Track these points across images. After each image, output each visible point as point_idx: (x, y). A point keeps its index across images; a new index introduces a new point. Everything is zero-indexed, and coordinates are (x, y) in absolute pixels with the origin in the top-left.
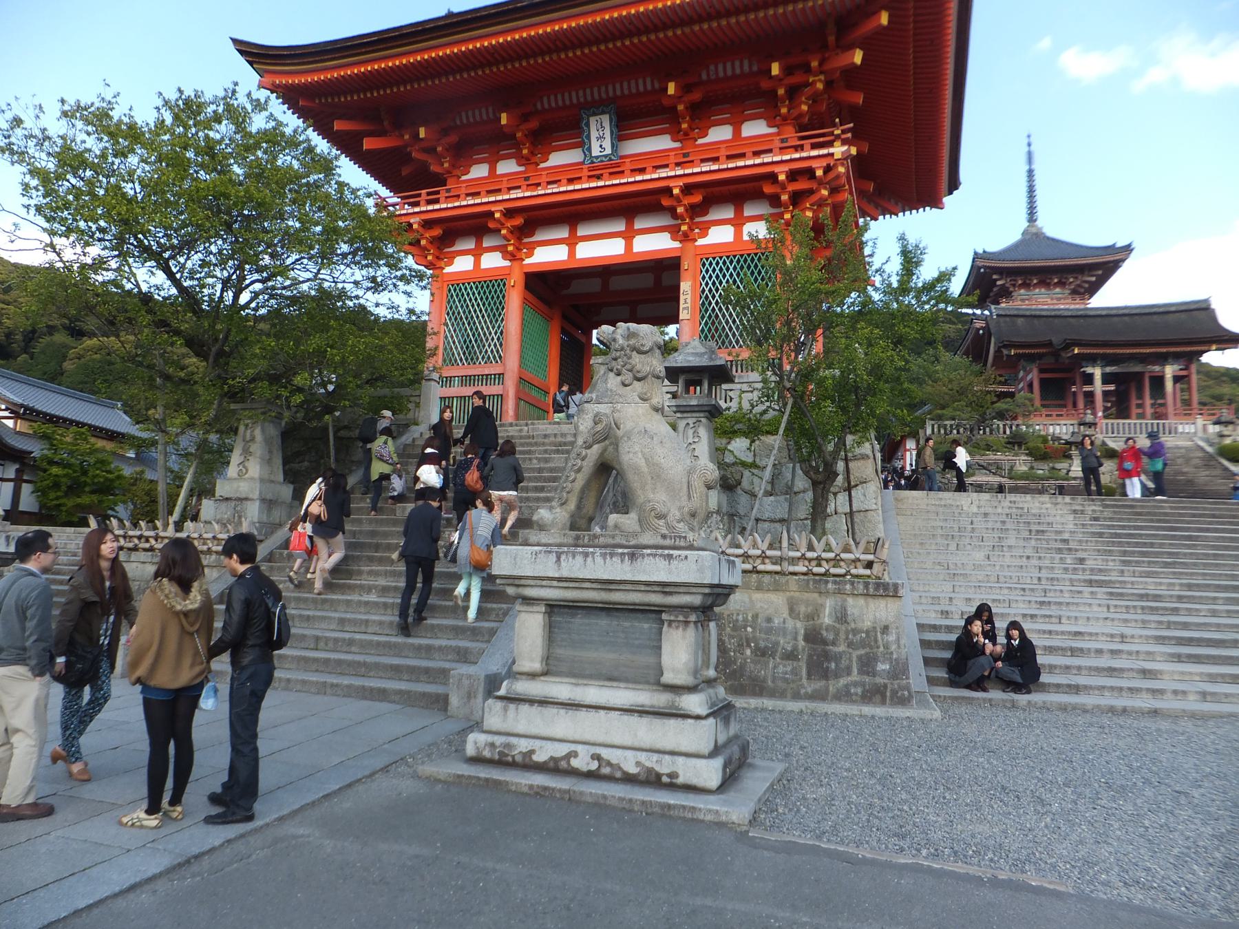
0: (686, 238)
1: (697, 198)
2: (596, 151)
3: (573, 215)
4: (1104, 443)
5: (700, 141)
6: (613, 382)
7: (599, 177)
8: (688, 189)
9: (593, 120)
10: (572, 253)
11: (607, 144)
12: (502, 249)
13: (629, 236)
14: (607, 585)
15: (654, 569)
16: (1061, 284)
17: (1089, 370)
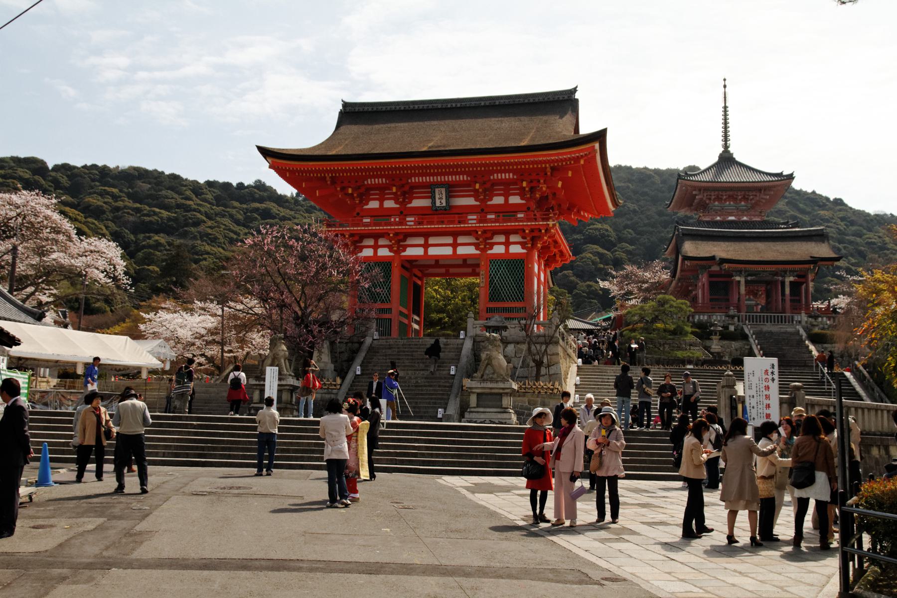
0: (484, 250)
1: (489, 235)
2: (438, 204)
3: (426, 235)
4: (742, 329)
5: (489, 203)
6: (490, 347)
7: (442, 223)
8: (485, 232)
9: (437, 190)
10: (426, 251)
11: (444, 201)
12: (390, 248)
13: (455, 245)
14: (491, 388)
15: (501, 385)
16: (745, 198)
17: (738, 278)
